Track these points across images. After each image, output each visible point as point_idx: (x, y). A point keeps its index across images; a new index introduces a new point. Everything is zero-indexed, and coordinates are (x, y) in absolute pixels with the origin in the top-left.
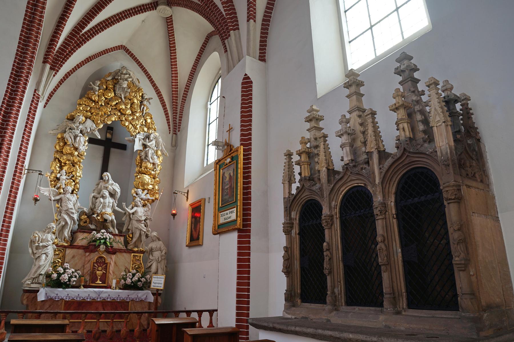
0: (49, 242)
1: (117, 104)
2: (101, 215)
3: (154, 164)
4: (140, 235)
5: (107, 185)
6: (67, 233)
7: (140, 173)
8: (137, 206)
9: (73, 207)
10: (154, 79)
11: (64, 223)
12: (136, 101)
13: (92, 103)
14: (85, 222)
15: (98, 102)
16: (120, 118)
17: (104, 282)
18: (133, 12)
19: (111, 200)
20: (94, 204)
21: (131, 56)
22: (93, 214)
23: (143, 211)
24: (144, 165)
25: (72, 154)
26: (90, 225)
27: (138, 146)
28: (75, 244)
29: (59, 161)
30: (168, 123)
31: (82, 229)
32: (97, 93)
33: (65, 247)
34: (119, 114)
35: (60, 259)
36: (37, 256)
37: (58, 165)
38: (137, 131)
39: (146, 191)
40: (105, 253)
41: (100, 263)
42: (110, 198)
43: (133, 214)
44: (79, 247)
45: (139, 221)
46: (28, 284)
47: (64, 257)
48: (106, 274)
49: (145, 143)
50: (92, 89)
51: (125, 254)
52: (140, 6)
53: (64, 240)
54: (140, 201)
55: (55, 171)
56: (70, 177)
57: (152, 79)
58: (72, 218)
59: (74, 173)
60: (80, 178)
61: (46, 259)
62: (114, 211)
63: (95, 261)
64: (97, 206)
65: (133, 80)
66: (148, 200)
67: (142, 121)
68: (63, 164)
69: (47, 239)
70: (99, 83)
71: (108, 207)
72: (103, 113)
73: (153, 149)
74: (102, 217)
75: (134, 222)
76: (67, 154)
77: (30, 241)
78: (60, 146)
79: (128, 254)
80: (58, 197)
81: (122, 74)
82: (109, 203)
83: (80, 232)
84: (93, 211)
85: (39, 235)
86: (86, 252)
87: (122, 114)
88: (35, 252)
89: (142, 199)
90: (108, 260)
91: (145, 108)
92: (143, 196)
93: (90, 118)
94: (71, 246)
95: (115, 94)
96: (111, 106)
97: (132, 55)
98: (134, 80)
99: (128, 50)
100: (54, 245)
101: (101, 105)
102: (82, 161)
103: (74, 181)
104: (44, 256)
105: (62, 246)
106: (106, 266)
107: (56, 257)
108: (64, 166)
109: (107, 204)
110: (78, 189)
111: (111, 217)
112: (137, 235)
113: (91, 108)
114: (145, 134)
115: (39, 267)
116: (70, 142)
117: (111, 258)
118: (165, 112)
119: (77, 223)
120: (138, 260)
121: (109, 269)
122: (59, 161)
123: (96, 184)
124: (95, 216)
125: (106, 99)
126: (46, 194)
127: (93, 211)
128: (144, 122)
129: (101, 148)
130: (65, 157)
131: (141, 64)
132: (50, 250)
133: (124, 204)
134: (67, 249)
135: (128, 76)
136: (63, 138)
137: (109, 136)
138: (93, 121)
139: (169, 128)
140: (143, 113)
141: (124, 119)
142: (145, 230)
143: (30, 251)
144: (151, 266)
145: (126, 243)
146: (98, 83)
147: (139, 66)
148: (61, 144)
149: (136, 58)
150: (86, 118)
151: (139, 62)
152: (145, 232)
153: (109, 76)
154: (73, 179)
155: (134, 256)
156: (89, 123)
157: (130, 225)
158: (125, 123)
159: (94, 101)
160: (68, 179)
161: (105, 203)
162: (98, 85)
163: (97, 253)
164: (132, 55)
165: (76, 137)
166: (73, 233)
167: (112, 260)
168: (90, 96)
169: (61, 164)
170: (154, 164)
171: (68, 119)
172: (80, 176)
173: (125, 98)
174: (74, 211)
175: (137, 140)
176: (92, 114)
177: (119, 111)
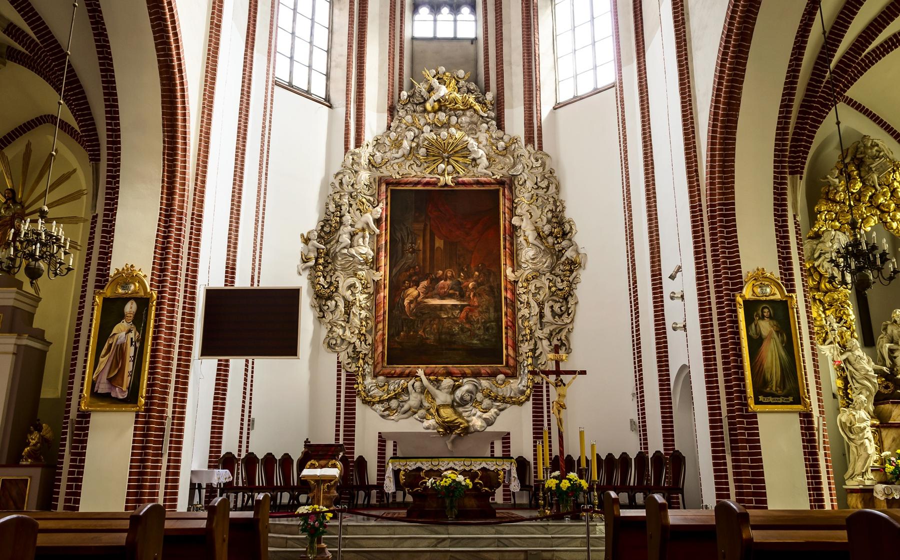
1: (871, 197)
16: (881, 219)
21: (857, 109)
34: (879, 213)
37: (821, 308)
87: (883, 212)
95: (864, 183)
113: (836, 214)
147: (875, 121)
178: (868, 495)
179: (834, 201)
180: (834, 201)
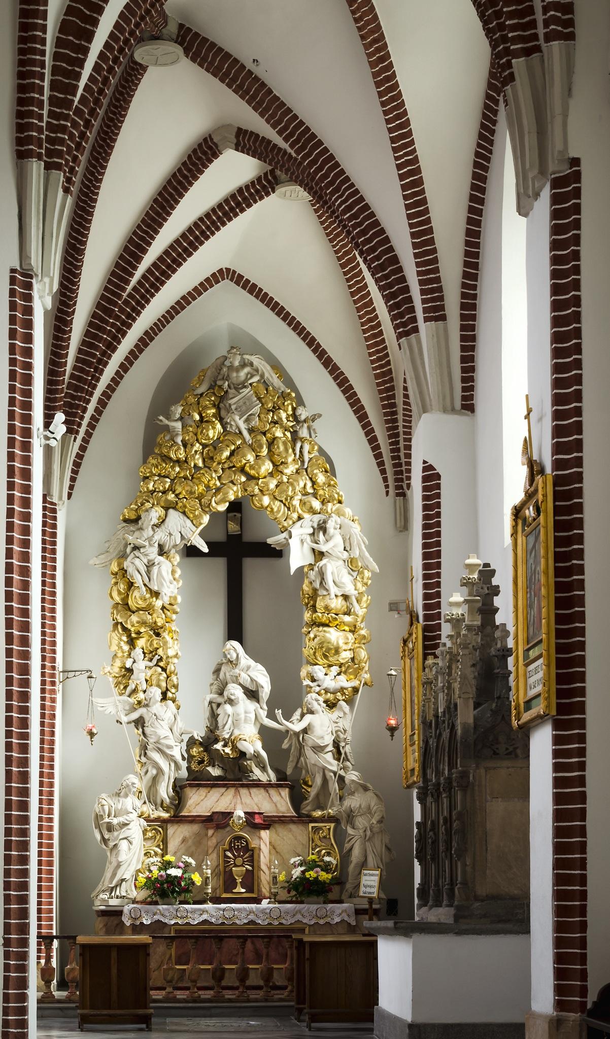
0: (130, 815)
1: (232, 453)
2: (233, 743)
3: (346, 597)
4: (325, 781)
5: (237, 671)
6: (165, 791)
7: (315, 624)
8: (312, 712)
9: (169, 733)
10: (324, 346)
11: (154, 772)
12: (279, 433)
13: (173, 467)
14: (201, 762)
15: (186, 461)
17: (250, 890)
18: (219, 218)
19: (251, 706)
20: (214, 716)
22: (216, 741)
23: (327, 723)
24: (320, 604)
25: (149, 609)
26: (210, 769)
27: (298, 557)
28: (184, 813)
29: (125, 629)
30: (381, 464)
31: (198, 778)
32: (179, 440)
33: (164, 822)
34: (243, 479)
35: (158, 846)
36: (111, 844)
37: (125, 638)
38: (295, 516)
39: (335, 670)
40: (248, 828)
41: (238, 850)
42: (248, 702)
43: (305, 731)
44: (192, 820)
45: (318, 749)
46: (103, 900)
47: (165, 841)
48: (252, 871)
49: (315, 546)
50: (167, 429)
51: (293, 827)
52: (233, 196)
53: (162, 806)
54: (317, 700)
55: (120, 654)
56: (155, 661)
57: (319, 345)
58: (170, 758)
59: (160, 652)
60: (175, 660)
61: (130, 849)
62: (265, 733)
63: (226, 847)
64: (220, 724)
65: (262, 376)
66: (342, 690)
67: (302, 484)
68: (133, 635)
69: (126, 809)
70: (180, 409)
71: (246, 721)
72: (202, 488)
73: (338, 558)
74: (234, 748)
75: (309, 752)
76: (139, 609)
77: (93, 816)
78: (119, 593)
79: (301, 827)
80: (135, 716)
81: (231, 368)
82: (246, 712)
83: (191, 786)
84: (212, 737)
85: (108, 802)
86: (207, 829)
88: (106, 837)
89: (327, 691)
90: (254, 844)
91: (307, 447)
92: (329, 682)
93: (174, 508)
94: (177, 818)
96: (219, 463)
97: (253, 289)
98: (266, 375)
99: (241, 277)
100: (142, 820)
101: (195, 465)
102: (174, 617)
103: (164, 670)
104: (124, 845)
105: (157, 819)
106: (252, 856)
107: (149, 843)
108: (137, 638)
109: (242, 716)
110: (176, 687)
111: (252, 744)
112: (319, 780)
113: (173, 480)
114: (316, 518)
115: (119, 866)
116: (138, 580)
117: (260, 838)
118: (367, 434)
119: (184, 764)
120: (325, 837)
121: (259, 861)
122: (125, 629)
123: (213, 669)
124: (219, 746)
125: (204, 446)
126: (111, 709)
127: (212, 737)
128: (309, 484)
129: (219, 565)
130: (134, 618)
131: (283, 308)
132: (136, 829)
133: (279, 713)
134: (169, 825)
135: (247, 370)
136: (123, 572)
137: (233, 527)
138: (184, 513)
139: (385, 480)
140: (303, 462)
141: (257, 491)
142: (335, 769)
143: (98, 837)
144: (351, 849)
145: (297, 799)
146: (178, 410)
148: (122, 587)
149: (266, 294)
150: (166, 509)
151: (277, 304)
152: (335, 773)
153: (201, 382)
154: (161, 664)
155: (316, 830)
156: (175, 519)
157: (302, 759)
158: (260, 500)
159: (178, 461)
160: (150, 668)
161: (238, 715)
162: (178, 416)
163: (228, 829)
164: (253, 289)
165: (150, 566)
166: (179, 788)
167: (264, 840)
168: (165, 451)
169: (129, 636)
170: (346, 597)
171: (126, 521)
172: (176, 656)
173: (251, 431)
174: (171, 742)
175: (294, 543)
176: (177, 496)
177: (242, 470)
178: (114, 920)
179: (166, 458)
180: (166, 458)
